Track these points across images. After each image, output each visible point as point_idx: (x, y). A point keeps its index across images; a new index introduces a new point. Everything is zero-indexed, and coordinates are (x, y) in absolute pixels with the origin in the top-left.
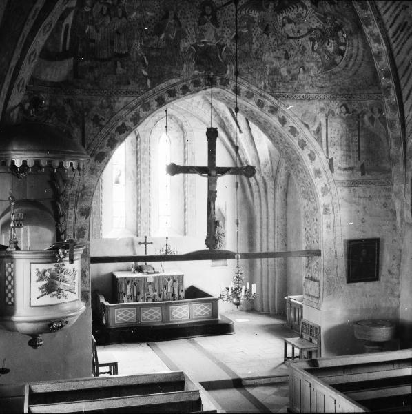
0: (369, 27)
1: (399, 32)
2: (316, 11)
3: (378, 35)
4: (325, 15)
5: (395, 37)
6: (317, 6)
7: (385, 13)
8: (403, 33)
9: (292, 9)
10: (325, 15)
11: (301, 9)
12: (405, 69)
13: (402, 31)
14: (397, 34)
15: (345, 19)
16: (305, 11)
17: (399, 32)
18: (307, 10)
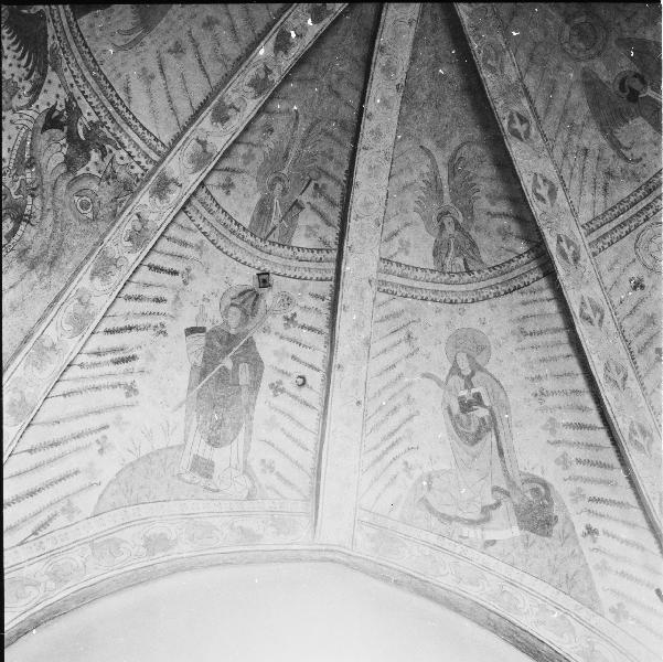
0: (97, 280)
1: (109, 357)
2: (33, 130)
3: (92, 316)
4: (31, 163)
5: (95, 359)
6: (45, 129)
7: (129, 298)
8: (113, 368)
9: (24, 62)
10: (31, 163)
11: (28, 86)
12: (50, 439)
13: (116, 362)
14: (102, 359)
15: (50, 218)
16: (25, 101)
17: (109, 357)
18: (28, 107)
